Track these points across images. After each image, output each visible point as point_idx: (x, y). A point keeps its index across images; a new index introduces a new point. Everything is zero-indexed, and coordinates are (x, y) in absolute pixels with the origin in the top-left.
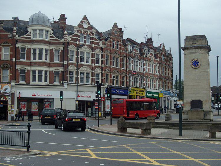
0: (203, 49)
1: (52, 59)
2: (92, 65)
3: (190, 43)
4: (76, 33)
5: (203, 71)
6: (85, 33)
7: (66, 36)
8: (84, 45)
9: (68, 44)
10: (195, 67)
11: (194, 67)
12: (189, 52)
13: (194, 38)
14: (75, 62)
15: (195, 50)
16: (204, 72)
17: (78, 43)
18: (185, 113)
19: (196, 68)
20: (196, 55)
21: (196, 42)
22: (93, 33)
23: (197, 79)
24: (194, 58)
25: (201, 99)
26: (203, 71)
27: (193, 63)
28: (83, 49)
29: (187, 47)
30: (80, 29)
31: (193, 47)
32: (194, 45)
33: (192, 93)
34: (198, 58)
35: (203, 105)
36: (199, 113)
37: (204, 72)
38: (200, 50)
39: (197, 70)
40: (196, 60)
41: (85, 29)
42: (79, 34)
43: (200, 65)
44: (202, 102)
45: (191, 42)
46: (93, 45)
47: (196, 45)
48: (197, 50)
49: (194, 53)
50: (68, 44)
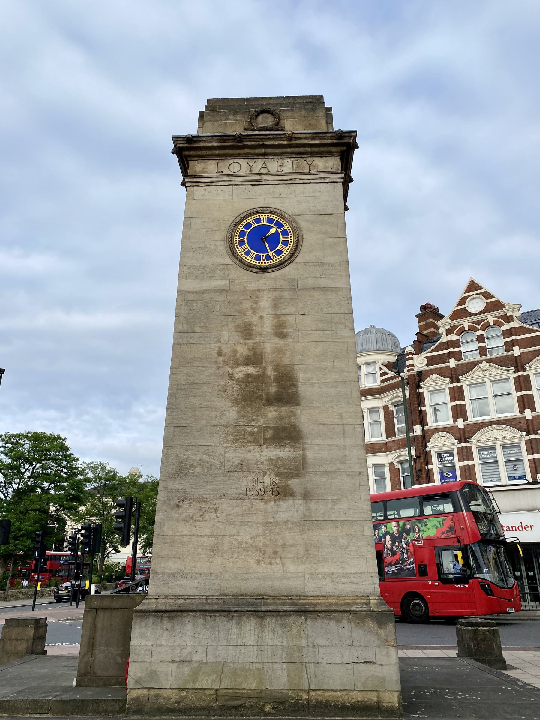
1: (390, 431)
2: (522, 415)
4: (445, 339)
6: (479, 327)
7: (412, 359)
8: (481, 362)
9: (421, 376)
14: (452, 422)
17: (452, 363)
22: (509, 314)
28: (474, 375)
30: (456, 322)
41: (477, 314)
42: (454, 337)
46: (517, 351)
50: (421, 376)
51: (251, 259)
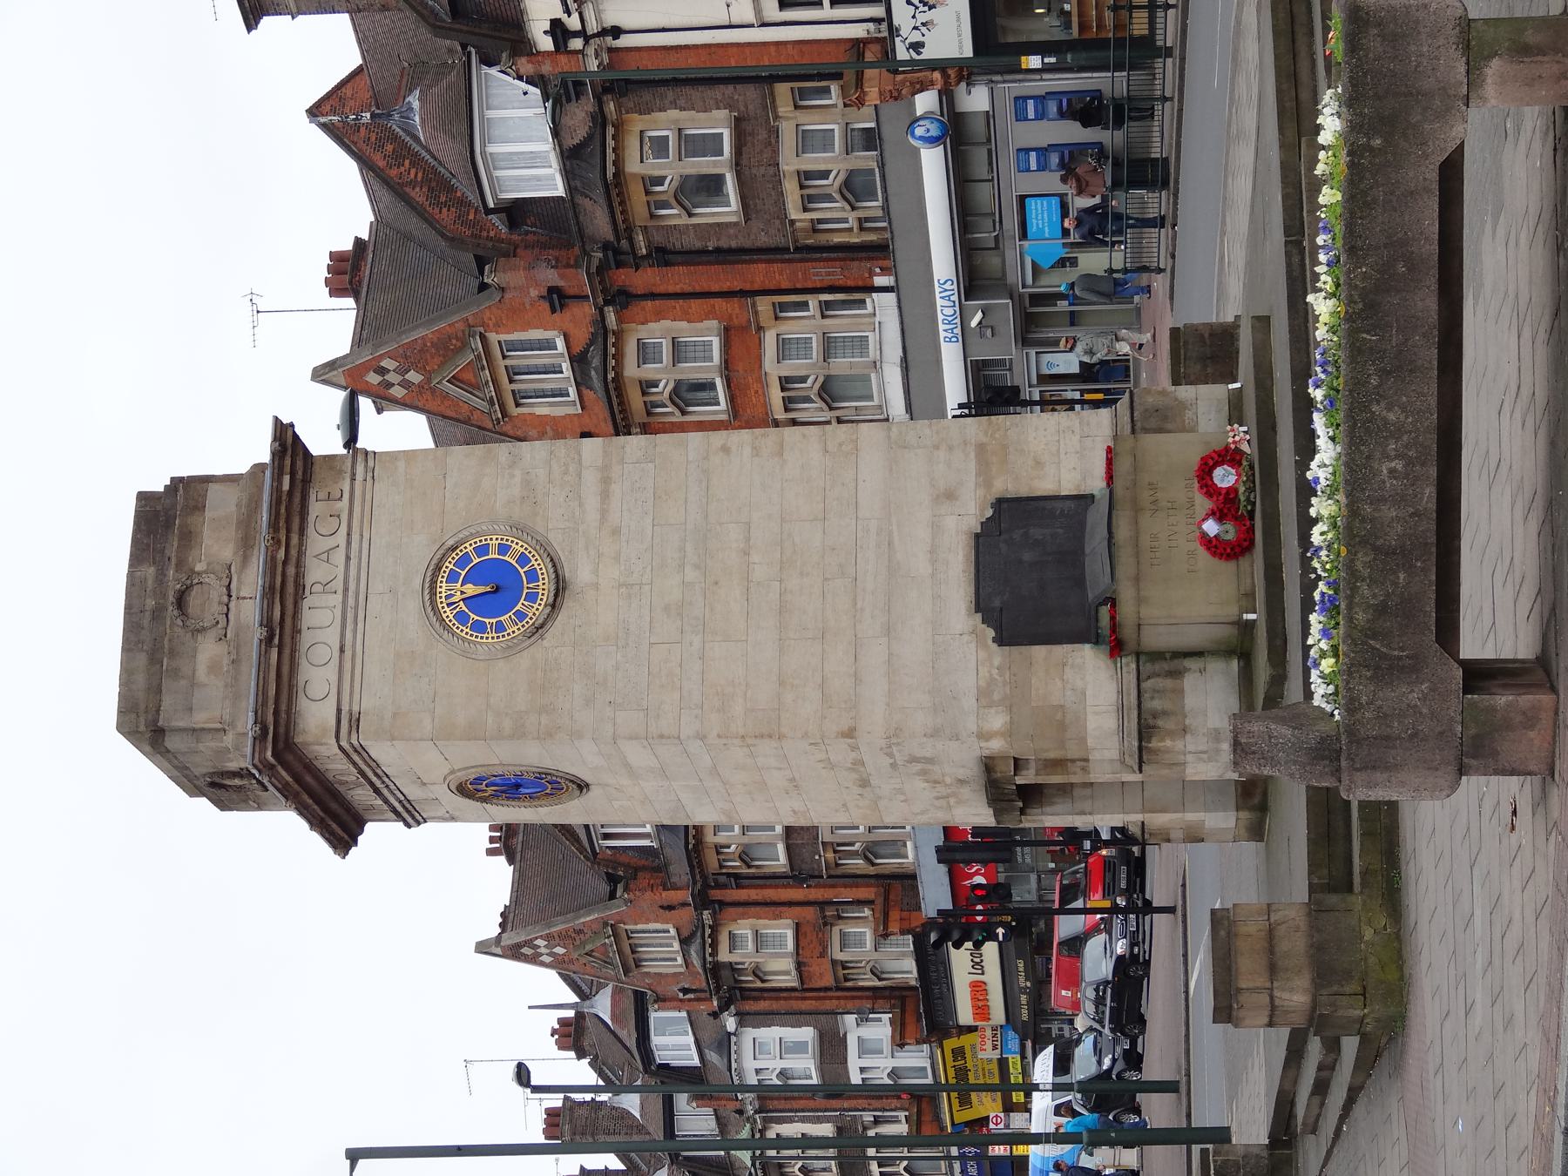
0: (316, 508)
3: (214, 668)
5: (592, 502)
10: (532, 597)
11: (537, 610)
12: (331, 673)
13: (158, 613)
15: (306, 604)
16: (606, 481)
18: (1157, 704)
19: (545, 587)
20: (377, 586)
21: (216, 591)
23: (691, 575)
24: (413, 605)
25: (971, 512)
26: (605, 495)
27: (479, 627)
29: (262, 692)
31: (267, 623)
32: (248, 612)
33: (888, 630)
34: (421, 552)
35: (1045, 485)
36: (1152, 486)
37: (606, 481)
38: (316, 543)
39: (580, 572)
40: (443, 588)
43: (519, 529)
44: (1001, 504)
45: (208, 650)
47: (251, 582)
48: (315, 572)
49: (352, 614)
51: (534, 610)
